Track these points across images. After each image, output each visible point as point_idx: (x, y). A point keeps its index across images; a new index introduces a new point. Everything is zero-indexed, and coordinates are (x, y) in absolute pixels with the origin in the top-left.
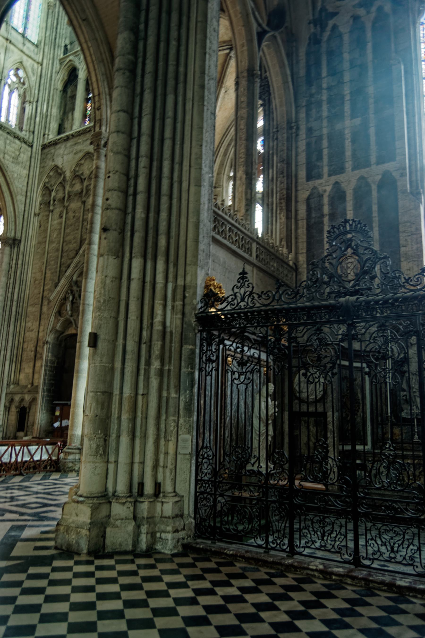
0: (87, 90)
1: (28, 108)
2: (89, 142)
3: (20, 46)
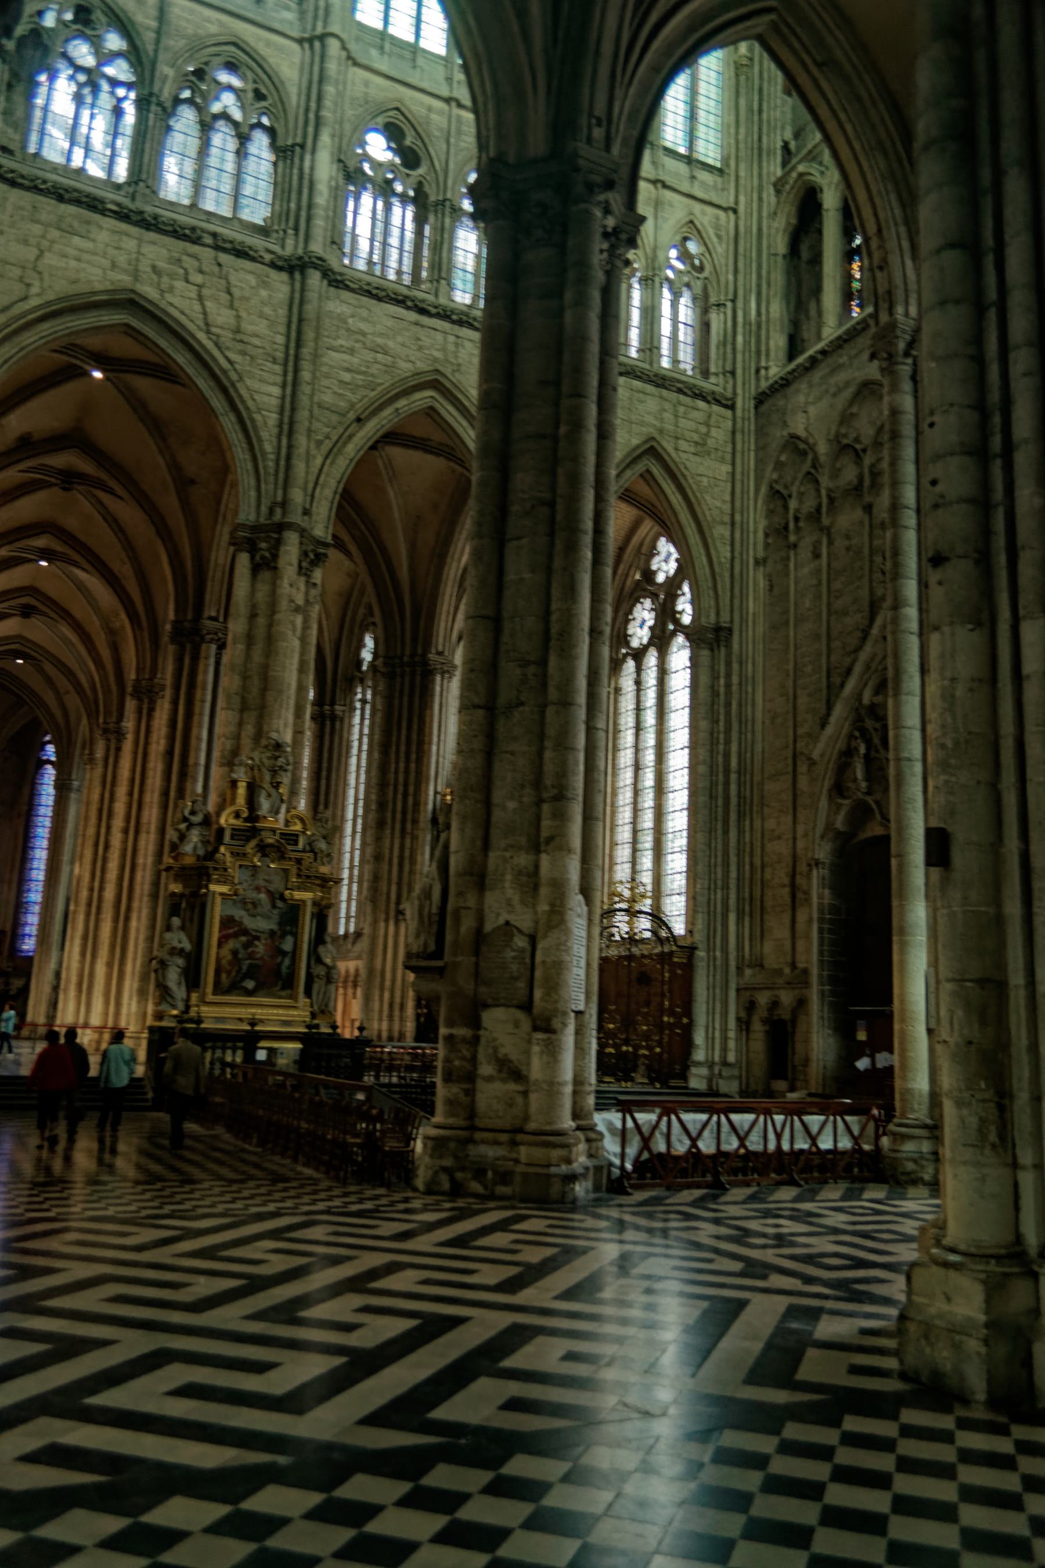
0: (848, 233)
1: (716, 320)
2: (866, 356)
3: (685, 187)
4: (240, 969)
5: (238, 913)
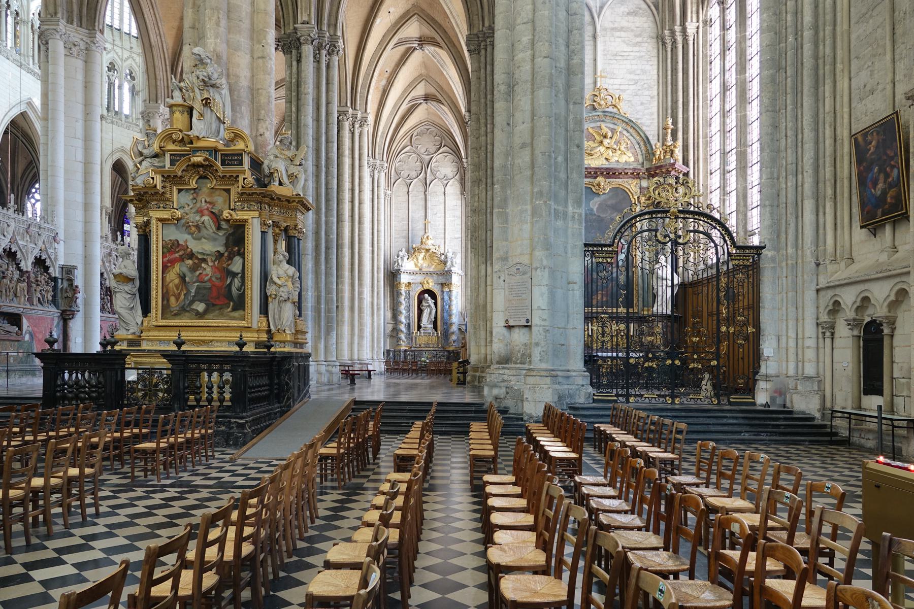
4: (188, 292)
5: (183, 237)
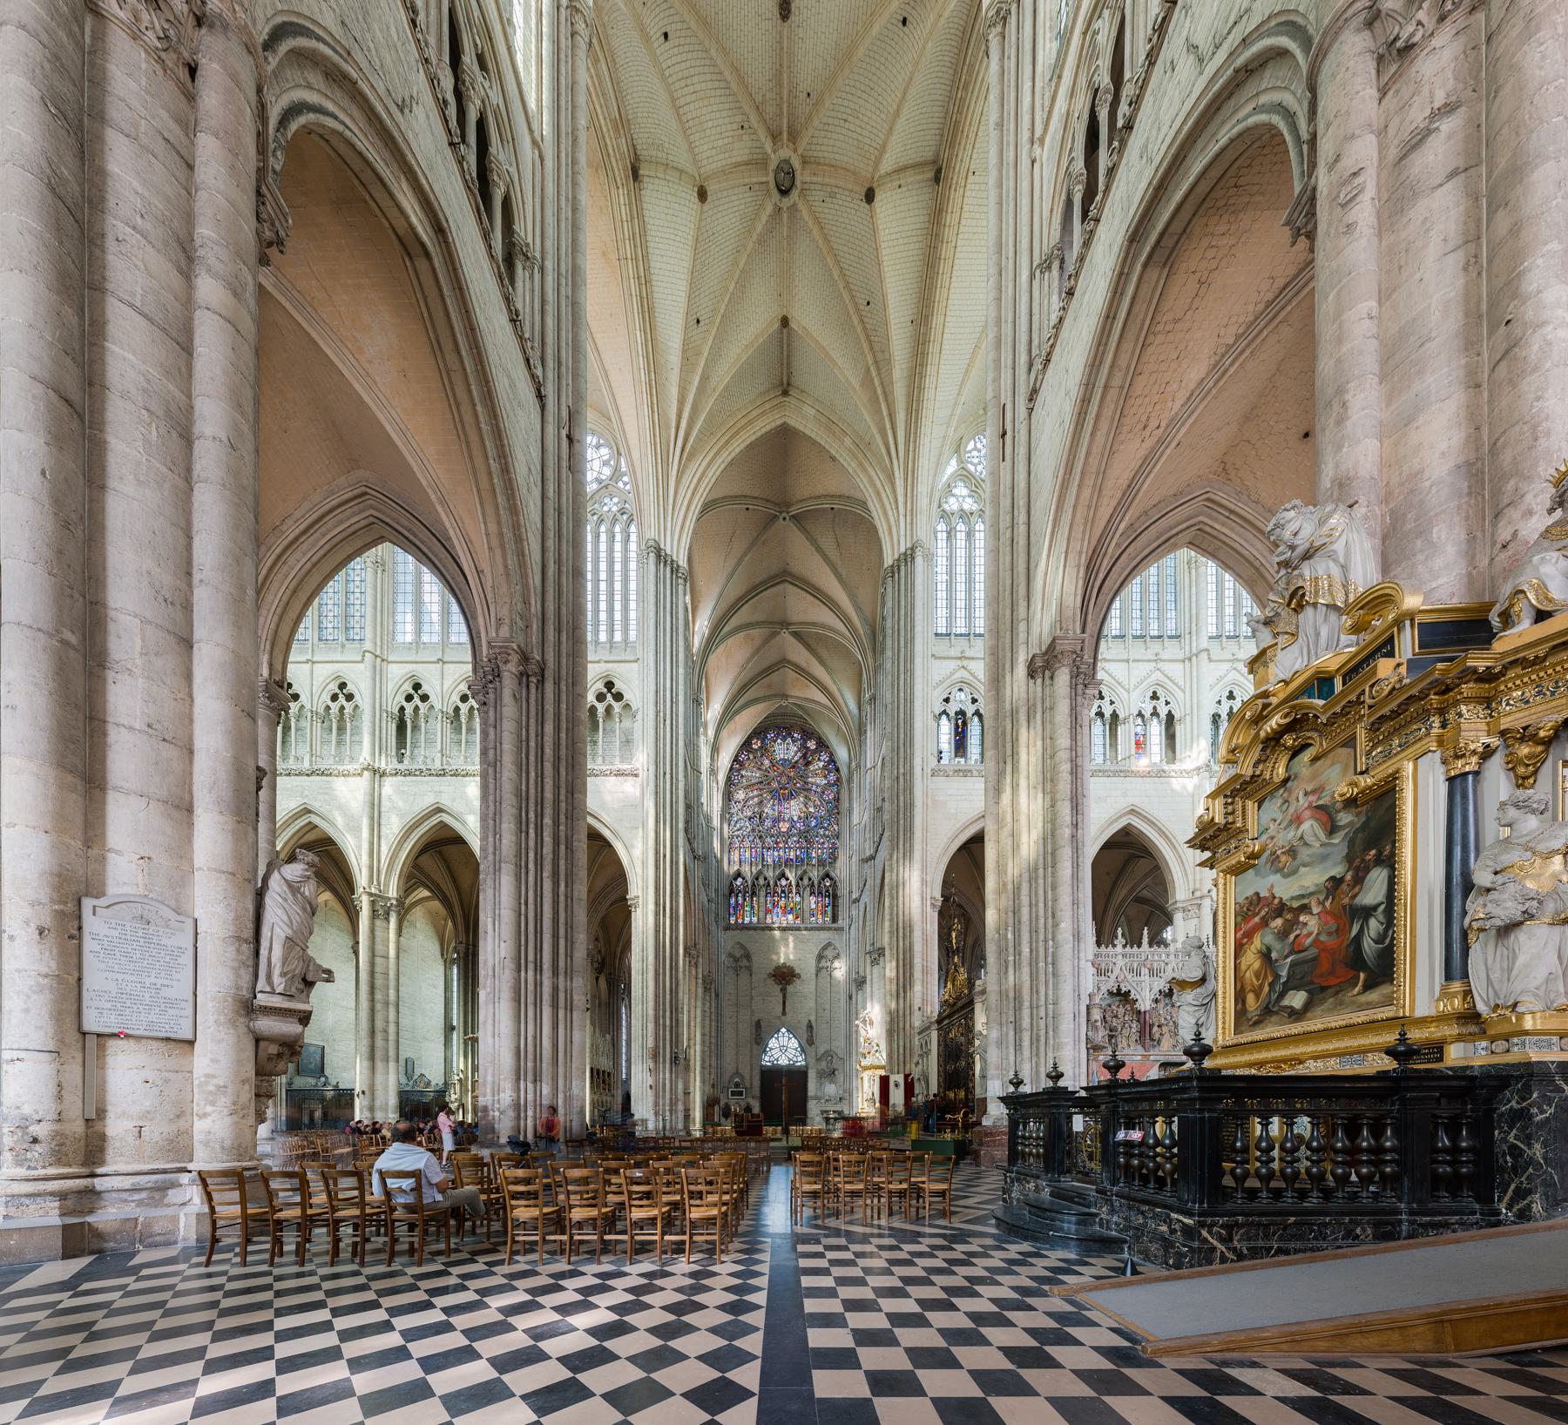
4: (1277, 976)
